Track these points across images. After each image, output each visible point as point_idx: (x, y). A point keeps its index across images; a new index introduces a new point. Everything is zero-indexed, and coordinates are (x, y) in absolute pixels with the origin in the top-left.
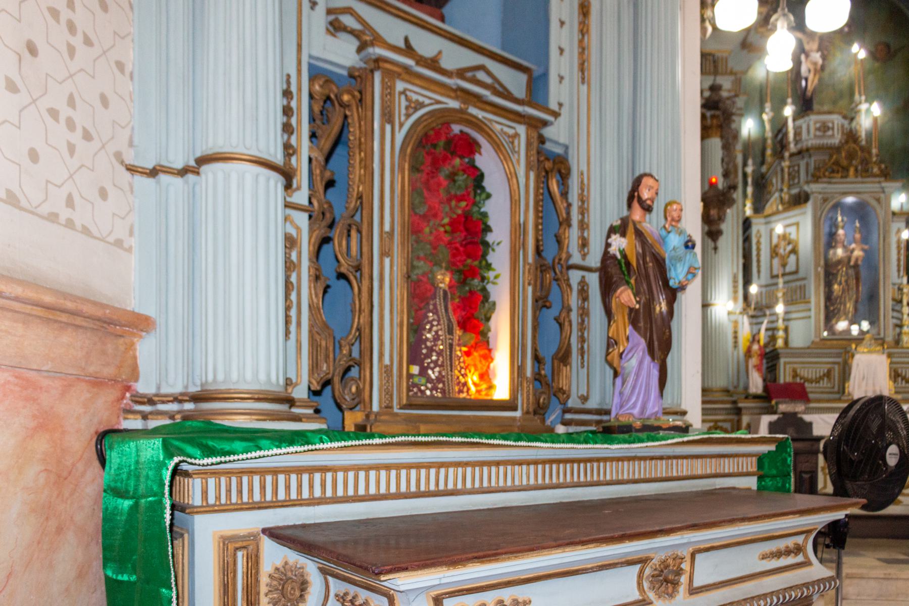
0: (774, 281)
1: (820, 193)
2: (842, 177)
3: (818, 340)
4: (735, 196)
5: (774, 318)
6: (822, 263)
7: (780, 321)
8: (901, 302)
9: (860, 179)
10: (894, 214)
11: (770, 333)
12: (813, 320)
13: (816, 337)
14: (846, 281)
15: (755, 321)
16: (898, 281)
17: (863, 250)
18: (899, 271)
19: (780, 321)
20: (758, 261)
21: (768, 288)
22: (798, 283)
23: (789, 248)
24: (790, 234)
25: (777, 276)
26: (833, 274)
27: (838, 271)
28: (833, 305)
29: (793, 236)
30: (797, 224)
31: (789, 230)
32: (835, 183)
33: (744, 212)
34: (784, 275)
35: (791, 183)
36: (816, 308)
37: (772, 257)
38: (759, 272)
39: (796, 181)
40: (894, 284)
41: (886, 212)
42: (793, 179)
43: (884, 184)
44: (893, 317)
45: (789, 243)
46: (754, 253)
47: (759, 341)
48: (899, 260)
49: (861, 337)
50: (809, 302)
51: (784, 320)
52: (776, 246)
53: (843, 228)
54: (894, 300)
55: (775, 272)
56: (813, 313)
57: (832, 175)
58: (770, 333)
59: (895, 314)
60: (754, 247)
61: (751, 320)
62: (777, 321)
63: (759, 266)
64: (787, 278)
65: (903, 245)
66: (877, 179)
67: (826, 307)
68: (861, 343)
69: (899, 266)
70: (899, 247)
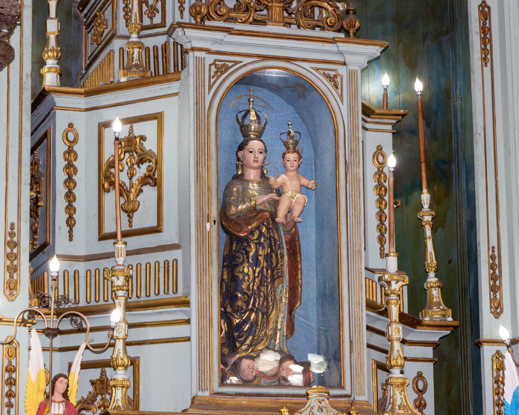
0: (107, 246)
1: (208, 51)
2: (256, 22)
3: (207, 394)
4: (14, 41)
5: (102, 338)
6: (214, 213)
7: (120, 345)
8: (385, 313)
9: (294, 30)
10: (367, 111)
11: (95, 374)
12: (194, 339)
13: (201, 389)
14: (268, 257)
15: (59, 341)
16: (376, 262)
17: (303, 189)
18: (381, 240)
19: (120, 345)
20: (70, 196)
21: (93, 265)
22: (161, 257)
23: (142, 171)
24: (143, 138)
25: (113, 236)
26: (240, 240)
27: (252, 233)
28: (238, 310)
29: (150, 145)
30: (158, 117)
31: (139, 129)
32: (242, 33)
33: (41, 77)
34: (126, 234)
35: (147, 22)
36: (200, 316)
37: (102, 190)
38: (71, 223)
39: (158, 19)
40: (373, 271)
41: (351, 108)
42: (152, 11)
43: (343, 47)
44: (369, 346)
45: (141, 161)
46: (61, 176)
47: (65, 395)
48: (381, 215)
49: (303, 392)
50: (187, 303)
51: (127, 344)
52: (111, 165)
53: (259, 137)
54: (371, 306)
55: (109, 228)
56: (192, 330)
57: (233, 15)
58: (95, 374)
59: (377, 340)
60: (60, 163)
61: (47, 340)
62: (113, 345)
63: (70, 209)
64: (135, 242)
65: (389, 183)
66: (330, 34)
67: (225, 315)
68: (304, 404)
69: (381, 228)
70: (380, 186)
